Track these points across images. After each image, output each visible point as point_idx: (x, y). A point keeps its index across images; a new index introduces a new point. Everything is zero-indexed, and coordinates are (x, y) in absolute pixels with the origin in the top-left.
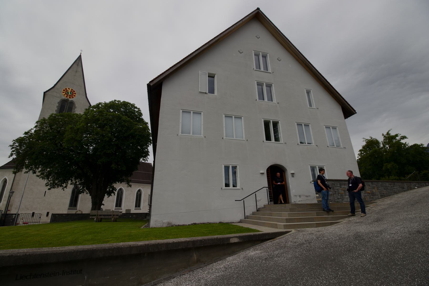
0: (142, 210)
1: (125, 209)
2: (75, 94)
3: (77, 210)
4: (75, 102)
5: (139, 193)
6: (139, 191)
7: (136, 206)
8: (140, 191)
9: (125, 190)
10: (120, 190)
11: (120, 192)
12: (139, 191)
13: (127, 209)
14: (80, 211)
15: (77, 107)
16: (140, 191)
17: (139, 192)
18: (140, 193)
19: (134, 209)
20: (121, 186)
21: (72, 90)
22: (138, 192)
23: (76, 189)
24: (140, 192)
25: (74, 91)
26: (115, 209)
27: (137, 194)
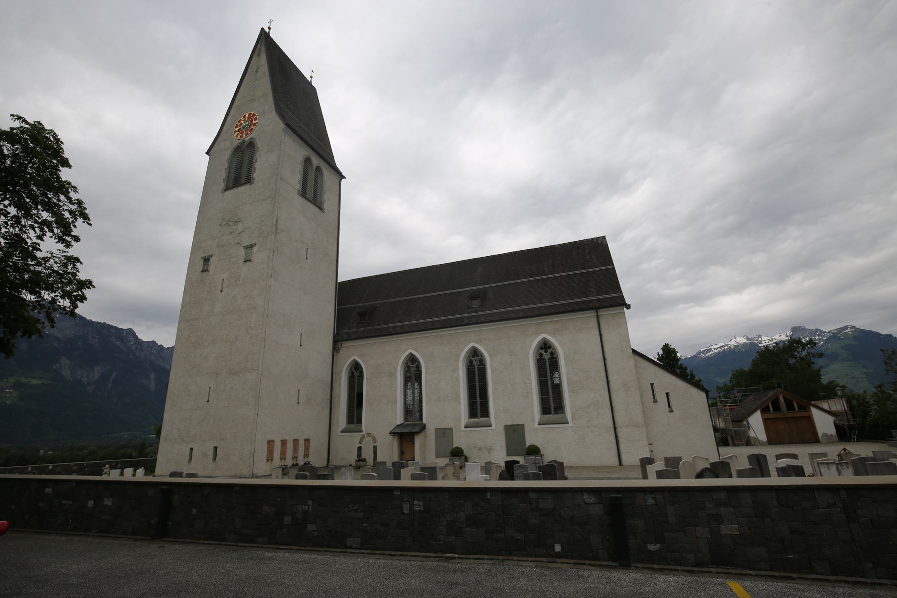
0: (570, 424)
1: (503, 425)
2: (256, 119)
3: (362, 432)
4: (256, 139)
5: (547, 356)
6: (545, 346)
7: (545, 410)
8: (550, 347)
9: (488, 351)
10: (473, 356)
11: (476, 364)
12: (545, 346)
13: (510, 423)
14: (371, 434)
15: (260, 149)
16: (550, 347)
17: (546, 352)
18: (552, 354)
19: (537, 421)
20: (470, 342)
21: (250, 114)
22: (543, 352)
23: (356, 371)
24: (549, 351)
25: (254, 115)
26: (465, 427)
27: (540, 363)
